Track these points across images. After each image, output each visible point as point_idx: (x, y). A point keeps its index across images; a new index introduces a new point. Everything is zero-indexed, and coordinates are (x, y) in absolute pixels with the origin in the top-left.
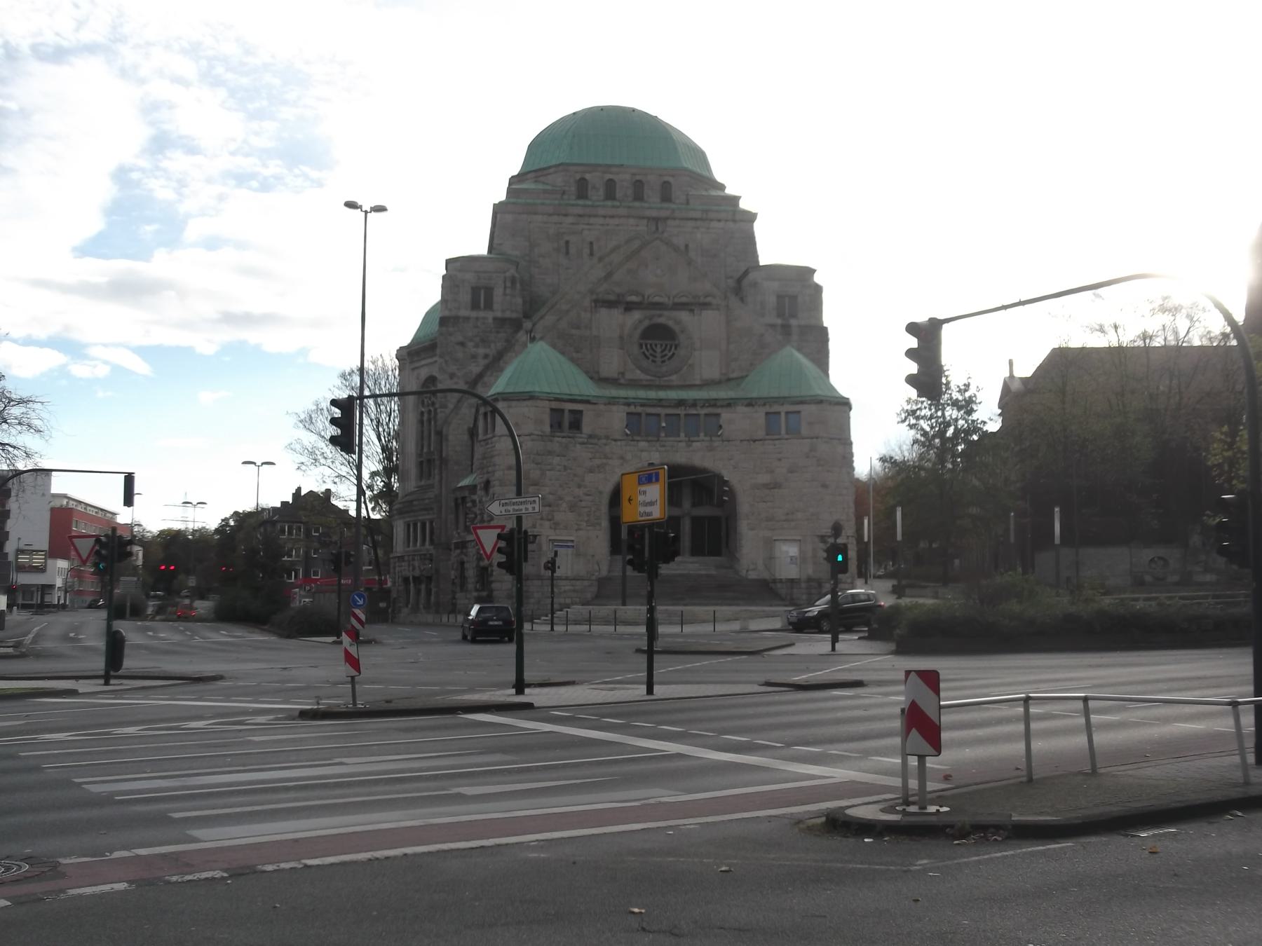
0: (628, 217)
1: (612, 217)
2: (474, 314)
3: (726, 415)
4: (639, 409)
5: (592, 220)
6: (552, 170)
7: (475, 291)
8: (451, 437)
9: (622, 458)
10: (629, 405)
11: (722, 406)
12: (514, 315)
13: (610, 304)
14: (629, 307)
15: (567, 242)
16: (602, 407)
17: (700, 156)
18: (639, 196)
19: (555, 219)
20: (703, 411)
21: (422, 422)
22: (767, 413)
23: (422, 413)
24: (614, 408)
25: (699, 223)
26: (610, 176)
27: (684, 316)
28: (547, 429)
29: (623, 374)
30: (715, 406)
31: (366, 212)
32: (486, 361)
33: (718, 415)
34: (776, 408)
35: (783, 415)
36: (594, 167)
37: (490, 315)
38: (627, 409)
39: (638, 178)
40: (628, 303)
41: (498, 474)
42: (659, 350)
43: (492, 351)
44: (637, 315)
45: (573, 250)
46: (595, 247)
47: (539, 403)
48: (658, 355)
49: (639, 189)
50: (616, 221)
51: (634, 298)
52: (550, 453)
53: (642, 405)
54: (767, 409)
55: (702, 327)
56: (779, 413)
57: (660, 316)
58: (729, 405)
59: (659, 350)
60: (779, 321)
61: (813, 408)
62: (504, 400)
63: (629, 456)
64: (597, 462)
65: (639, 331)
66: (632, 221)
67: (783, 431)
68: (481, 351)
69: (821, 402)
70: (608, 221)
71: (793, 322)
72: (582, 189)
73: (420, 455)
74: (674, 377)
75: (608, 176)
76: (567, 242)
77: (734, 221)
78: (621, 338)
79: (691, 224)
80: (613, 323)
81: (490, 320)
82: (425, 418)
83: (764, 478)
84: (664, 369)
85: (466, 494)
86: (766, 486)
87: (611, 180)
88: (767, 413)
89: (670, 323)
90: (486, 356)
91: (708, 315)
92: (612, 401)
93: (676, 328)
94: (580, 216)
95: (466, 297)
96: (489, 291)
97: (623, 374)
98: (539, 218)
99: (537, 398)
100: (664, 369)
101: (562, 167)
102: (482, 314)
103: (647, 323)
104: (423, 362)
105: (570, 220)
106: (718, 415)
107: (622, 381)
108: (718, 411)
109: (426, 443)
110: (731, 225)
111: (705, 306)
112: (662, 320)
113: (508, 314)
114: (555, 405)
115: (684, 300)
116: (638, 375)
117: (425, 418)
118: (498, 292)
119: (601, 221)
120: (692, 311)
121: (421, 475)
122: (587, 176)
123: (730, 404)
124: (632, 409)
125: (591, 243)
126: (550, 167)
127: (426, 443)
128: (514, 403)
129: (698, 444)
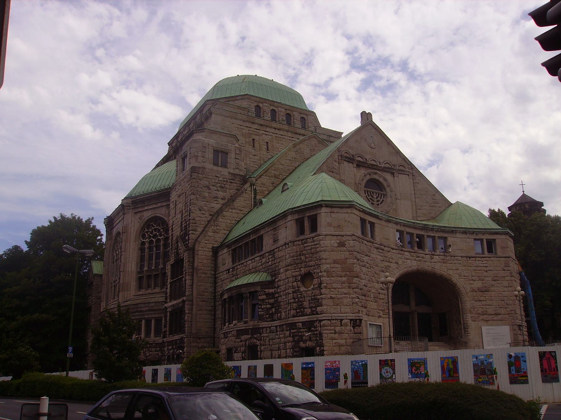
0: (287, 131)
1: (279, 129)
2: (215, 168)
4: (402, 228)
5: (268, 129)
6: (237, 98)
7: (216, 152)
8: (200, 253)
9: (397, 263)
11: (448, 232)
12: (242, 173)
14: (360, 165)
15: (254, 140)
16: (384, 223)
20: (437, 235)
21: (142, 250)
22: (475, 239)
23: (143, 243)
24: (390, 225)
27: (388, 176)
30: (444, 231)
32: (222, 202)
36: (266, 101)
37: (225, 172)
39: (288, 112)
41: (325, 267)
43: (227, 195)
44: (363, 171)
45: (256, 145)
46: (269, 145)
47: (355, 211)
48: (375, 200)
50: (282, 133)
54: (474, 236)
56: (482, 240)
57: (376, 173)
58: (452, 232)
59: (375, 197)
62: (327, 206)
65: (365, 182)
66: (290, 134)
68: (221, 194)
70: (277, 131)
73: (139, 273)
75: (272, 108)
76: (254, 140)
78: (355, 183)
81: (226, 174)
82: (147, 245)
83: (478, 284)
85: (258, 288)
86: (480, 290)
87: (273, 110)
89: (381, 180)
90: (223, 199)
93: (385, 184)
94: (261, 125)
102: (220, 169)
103: (368, 177)
104: (146, 208)
105: (256, 126)
106: (445, 239)
109: (146, 263)
111: (401, 172)
112: (376, 177)
113: (237, 172)
115: (387, 165)
117: (147, 245)
118: (232, 156)
119: (273, 131)
120: (393, 174)
121: (140, 287)
122: (261, 105)
125: (267, 143)
126: (237, 96)
127: (146, 263)
128: (335, 210)
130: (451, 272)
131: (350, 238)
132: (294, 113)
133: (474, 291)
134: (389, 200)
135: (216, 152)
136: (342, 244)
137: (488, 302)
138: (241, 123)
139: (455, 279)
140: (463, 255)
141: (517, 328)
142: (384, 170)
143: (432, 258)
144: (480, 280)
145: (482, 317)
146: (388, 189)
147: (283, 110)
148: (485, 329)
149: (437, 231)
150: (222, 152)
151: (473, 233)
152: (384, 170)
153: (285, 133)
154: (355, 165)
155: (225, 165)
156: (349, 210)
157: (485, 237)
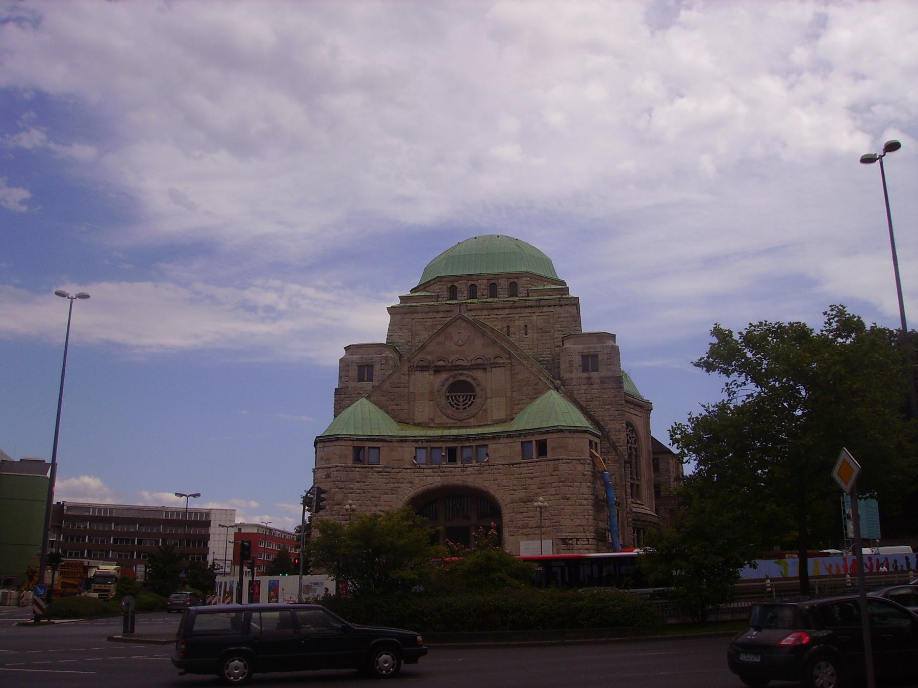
0: (481, 309)
3: (492, 446)
4: (425, 445)
7: (361, 367)
10: (417, 441)
11: (489, 439)
13: (423, 369)
14: (438, 370)
16: (395, 444)
17: (548, 263)
18: (493, 294)
19: (431, 315)
22: (522, 443)
24: (405, 445)
25: (534, 310)
26: (473, 283)
27: (479, 374)
28: (350, 463)
29: (433, 420)
30: (483, 439)
31: (72, 298)
33: (486, 446)
34: (528, 438)
35: (534, 443)
38: (416, 445)
39: (493, 281)
40: (436, 367)
42: (461, 400)
44: (444, 376)
47: (343, 443)
49: (493, 290)
51: (441, 363)
52: (352, 481)
53: (427, 441)
54: (522, 439)
55: (493, 381)
57: (461, 374)
58: (494, 438)
59: (461, 400)
60: (585, 375)
61: (555, 435)
63: (417, 480)
64: (392, 485)
65: (446, 386)
66: (485, 312)
67: (534, 456)
69: (561, 431)
71: (594, 375)
72: (453, 293)
74: (472, 420)
75: (470, 283)
77: (561, 306)
78: (432, 393)
79: (529, 310)
80: (424, 382)
83: (521, 494)
84: (465, 414)
86: (521, 500)
88: (522, 443)
89: (469, 379)
91: (497, 371)
92: (403, 440)
93: (473, 383)
95: (354, 372)
96: (371, 367)
97: (433, 420)
98: (419, 316)
99: (342, 439)
100: (465, 414)
101: (439, 279)
103: (451, 381)
105: (441, 315)
106: (486, 446)
107: (432, 425)
108: (486, 443)
110: (558, 308)
111: (494, 365)
114: (356, 444)
115: (479, 361)
116: (445, 420)
118: (377, 368)
122: (456, 284)
123: (495, 437)
124: (420, 445)
128: (327, 444)
129: (471, 469)
130: (487, 484)
131: (334, 469)
132: (500, 281)
133: (513, 502)
134: (478, 400)
135: (361, 367)
136: (328, 476)
137: (530, 514)
138: (424, 316)
139: (492, 489)
140: (504, 462)
141: (560, 542)
142: (469, 368)
143: (463, 471)
144: (523, 489)
145: (521, 531)
146: (478, 389)
147: (485, 281)
148: (522, 543)
149: (474, 440)
150: (367, 366)
151: (520, 436)
152: (469, 368)
153: (479, 313)
154: (432, 372)
155: (370, 379)
156: (336, 443)
157: (534, 439)
